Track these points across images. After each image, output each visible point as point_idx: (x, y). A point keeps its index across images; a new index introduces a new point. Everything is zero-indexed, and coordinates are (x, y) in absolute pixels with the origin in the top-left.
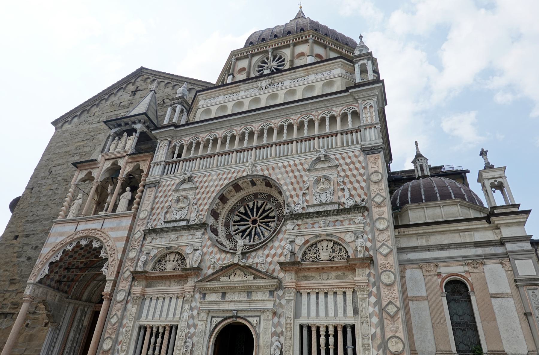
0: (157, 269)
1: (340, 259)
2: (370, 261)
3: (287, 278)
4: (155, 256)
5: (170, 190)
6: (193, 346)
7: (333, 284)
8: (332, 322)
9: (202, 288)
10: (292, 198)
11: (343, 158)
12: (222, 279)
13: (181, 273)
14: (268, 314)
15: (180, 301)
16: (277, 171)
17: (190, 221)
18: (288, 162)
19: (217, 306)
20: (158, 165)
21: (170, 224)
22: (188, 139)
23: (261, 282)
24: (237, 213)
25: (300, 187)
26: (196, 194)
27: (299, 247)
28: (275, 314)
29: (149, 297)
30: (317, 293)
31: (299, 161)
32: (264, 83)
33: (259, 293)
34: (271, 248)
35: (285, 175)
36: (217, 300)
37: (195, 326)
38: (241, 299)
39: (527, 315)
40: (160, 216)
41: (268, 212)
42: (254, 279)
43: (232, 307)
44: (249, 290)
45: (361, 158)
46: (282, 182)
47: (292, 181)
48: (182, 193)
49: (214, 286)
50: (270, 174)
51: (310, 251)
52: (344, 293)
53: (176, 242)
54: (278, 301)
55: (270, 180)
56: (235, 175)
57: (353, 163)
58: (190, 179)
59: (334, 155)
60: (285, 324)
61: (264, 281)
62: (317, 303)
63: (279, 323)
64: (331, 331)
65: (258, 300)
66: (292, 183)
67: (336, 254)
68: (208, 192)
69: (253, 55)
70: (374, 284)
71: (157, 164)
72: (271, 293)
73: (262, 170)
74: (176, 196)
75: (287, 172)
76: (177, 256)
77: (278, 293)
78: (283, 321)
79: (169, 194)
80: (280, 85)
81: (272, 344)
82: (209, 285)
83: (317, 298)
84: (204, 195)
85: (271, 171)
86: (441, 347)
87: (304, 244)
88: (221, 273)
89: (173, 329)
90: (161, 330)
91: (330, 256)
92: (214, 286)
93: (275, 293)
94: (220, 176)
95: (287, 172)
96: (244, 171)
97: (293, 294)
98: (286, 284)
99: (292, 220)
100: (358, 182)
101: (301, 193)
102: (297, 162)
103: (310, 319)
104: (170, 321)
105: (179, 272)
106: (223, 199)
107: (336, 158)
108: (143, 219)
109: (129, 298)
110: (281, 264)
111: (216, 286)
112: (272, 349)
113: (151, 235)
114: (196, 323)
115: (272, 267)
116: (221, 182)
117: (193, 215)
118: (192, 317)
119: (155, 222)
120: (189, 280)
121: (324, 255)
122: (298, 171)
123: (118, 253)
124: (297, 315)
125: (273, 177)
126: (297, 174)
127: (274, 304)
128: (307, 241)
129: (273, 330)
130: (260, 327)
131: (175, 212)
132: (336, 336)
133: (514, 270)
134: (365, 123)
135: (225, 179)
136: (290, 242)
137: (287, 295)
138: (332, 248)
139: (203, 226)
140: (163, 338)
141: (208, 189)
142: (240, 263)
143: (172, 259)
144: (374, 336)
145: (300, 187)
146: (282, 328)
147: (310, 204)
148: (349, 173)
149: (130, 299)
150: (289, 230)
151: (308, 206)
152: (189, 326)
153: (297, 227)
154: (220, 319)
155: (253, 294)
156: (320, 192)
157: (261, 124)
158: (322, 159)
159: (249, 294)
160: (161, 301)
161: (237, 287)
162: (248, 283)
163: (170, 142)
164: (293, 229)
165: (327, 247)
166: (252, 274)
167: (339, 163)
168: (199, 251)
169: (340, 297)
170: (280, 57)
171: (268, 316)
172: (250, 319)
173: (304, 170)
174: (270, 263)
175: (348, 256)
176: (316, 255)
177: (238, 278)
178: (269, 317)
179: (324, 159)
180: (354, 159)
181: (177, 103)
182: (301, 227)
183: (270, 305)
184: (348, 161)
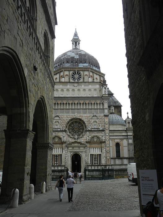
2: (105, 142)
8: (97, 153)
15: (61, 149)
16: (83, 117)
23: (82, 146)
28: (85, 152)
32: (76, 85)
37: (67, 155)
39: (129, 150)
45: (104, 117)
46: (85, 121)
48: (56, 120)
56: (72, 117)
57: (102, 118)
58: (58, 116)
64: (97, 155)
69: (70, 70)
70: (105, 147)
72: (84, 148)
73: (79, 117)
78: (87, 153)
80: (81, 86)
84: (63, 122)
86: (114, 156)
89: (61, 155)
90: (57, 155)
94: (67, 117)
104: (59, 153)
105: (60, 142)
106: (68, 123)
115: (84, 142)
116: (68, 118)
121: (95, 140)
124: (90, 152)
126: (88, 119)
132: (97, 156)
133: (128, 141)
139: (65, 131)
140: (58, 157)
144: (105, 156)
148: (101, 121)
169: (98, 149)
170: (79, 74)
177: (76, 145)
180: (102, 117)
183: (84, 150)
184: (101, 117)
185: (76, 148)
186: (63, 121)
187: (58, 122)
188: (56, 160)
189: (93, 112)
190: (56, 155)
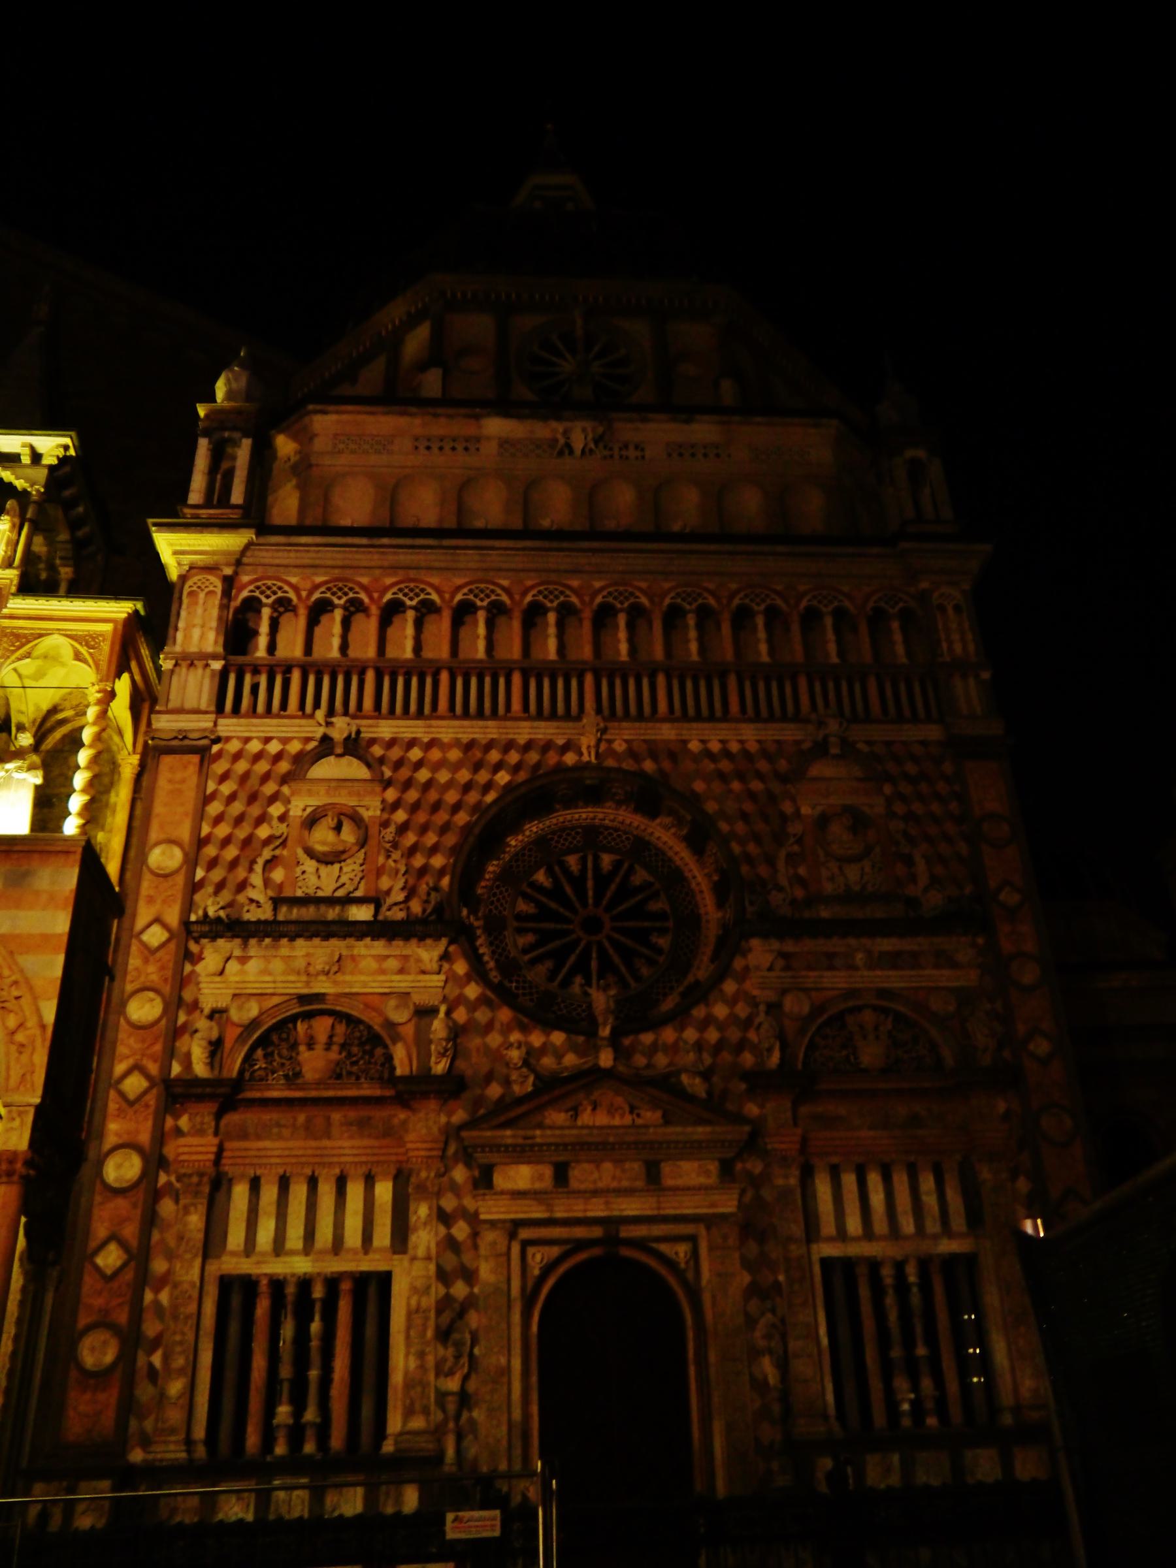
0: (262, 1073)
4: (254, 1023)
5: (266, 778)
17: (384, 908)
19: (543, 1208)
20: (192, 665)
21: (303, 911)
22: (308, 585)
23: (700, 1132)
24: (525, 887)
29: (243, 1176)
35: (717, 786)
36: (538, 1186)
37: (469, 1276)
38: (625, 1184)
40: (241, 873)
41: (639, 897)
43: (597, 1209)
45: (948, 768)
46: (711, 807)
49: (529, 1142)
53: (339, 977)
56: (533, 757)
59: (869, 743)
61: (708, 1129)
65: (688, 1189)
66: (745, 816)
68: (436, 807)
71: (190, 660)
74: (302, 806)
75: (722, 776)
76: (341, 1029)
77: (749, 1166)
79: (270, 788)
80: (632, 453)
84: (421, 817)
85: (667, 765)
90: (318, 1292)
92: (529, 1142)
93: (739, 1166)
95: (722, 776)
96: (565, 748)
97: (796, 1172)
101: (782, 854)
102: (753, 747)
108: (166, 876)
109: (163, 1179)
111: (538, 1140)
113: (221, 942)
116: (483, 777)
117: (394, 886)
118: (451, 1244)
119: (226, 896)
122: (760, 776)
123: (35, 999)
124: (812, 1232)
126: (756, 786)
127: (739, 1201)
131: (310, 865)
134: (948, 659)
135: (498, 767)
141: (433, 796)
142: (621, 1068)
143: (322, 1038)
149: (169, 1184)
152: (443, 1276)
153: (780, 963)
154: (555, 1251)
155: (666, 1168)
157: (602, 589)
160: (299, 1193)
163: (229, 583)
164: (770, 969)
172: (664, 1248)
176: (844, 1053)
181: (234, 429)
184: (911, 768)
185: (607, 1174)
190: (305, 1283)
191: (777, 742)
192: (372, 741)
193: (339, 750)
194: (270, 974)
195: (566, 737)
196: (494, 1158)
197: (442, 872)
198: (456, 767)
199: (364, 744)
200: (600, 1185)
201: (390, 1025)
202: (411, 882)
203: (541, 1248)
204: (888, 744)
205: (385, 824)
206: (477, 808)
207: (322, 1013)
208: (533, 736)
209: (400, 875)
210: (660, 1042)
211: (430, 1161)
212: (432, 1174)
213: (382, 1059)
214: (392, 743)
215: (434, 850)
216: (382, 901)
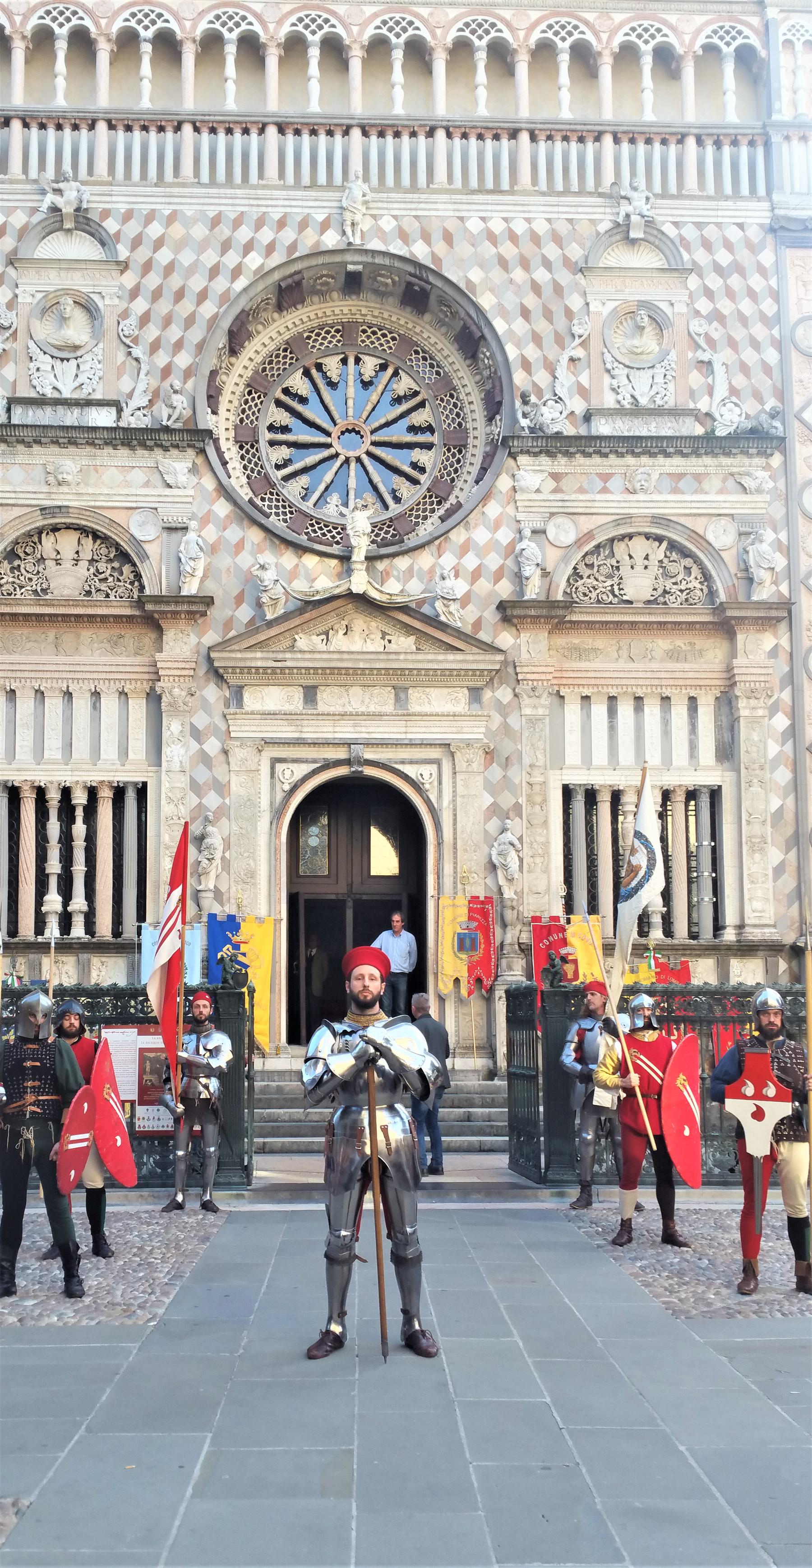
1: (687, 600)
3: (524, 650)
6: (227, 846)
7: (663, 675)
9: (233, 668)
10: (530, 373)
11: (707, 245)
12: (302, 642)
13: (128, 612)
14: (470, 754)
16: (463, 249)
17: (126, 412)
18: (506, 220)
19: (293, 728)
23: (451, 660)
25: (556, 333)
26: (127, 295)
27: (559, 553)
28: (490, 754)
30: (612, 699)
31: (547, 226)
33: (434, 693)
34: (465, 549)
35: (497, 275)
36: (287, 708)
37: (222, 789)
38: (372, 708)
42: (418, 649)
43: (346, 731)
44: (400, 683)
45: (767, 258)
46: (486, 301)
47: (526, 302)
50: (435, 258)
51: (590, 566)
52: (693, 700)
54: (497, 719)
55: (439, 283)
56: (288, 235)
59: (676, 224)
60: (524, 784)
61: (459, 657)
62: (612, 728)
63: (506, 783)
67: (675, 584)
68: (180, 295)
72: (475, 693)
73: (404, 236)
75: (503, 263)
78: (517, 775)
81: (490, 840)
82: (262, 659)
83: (612, 712)
84: (164, 306)
85: (440, 248)
87: (579, 542)
88: (297, 621)
90: (80, 798)
91: (655, 589)
92: (279, 664)
93: (487, 695)
94: (224, 231)
95: (503, 263)
96: (325, 226)
97: (545, 700)
98: (525, 670)
99: (536, 455)
100: (755, 345)
102: (541, 227)
103: (592, 772)
107: (682, 239)
110: (502, 606)
111: (289, 664)
112: (494, 852)
114: (223, 779)
116: (232, 259)
120: (164, 637)
122: (547, 264)
125: (454, 279)
126: (541, 275)
127: (487, 727)
128: (590, 535)
129: (488, 800)
130: (440, 791)
135: (248, 248)
136: (534, 532)
137: (526, 700)
138: (661, 562)
141: (175, 282)
145: (556, 333)
146: (515, 796)
147: (595, 404)
148: (725, 306)
150: (523, 490)
151: (587, 418)
152: (196, 787)
153: (551, 484)
154: (306, 769)
155: (414, 694)
156: (627, 363)
158: (633, 235)
159: (402, 696)
160: (54, 705)
161: (363, 669)
162: (405, 660)
164: (538, 491)
165: (647, 558)
166: (409, 630)
167: (694, 263)
168: (191, 536)
169: (679, 712)
171: (469, 762)
173: (567, 262)
174: (465, 601)
175: (712, 594)
176: (609, 583)
178: (475, 766)
179: (641, 235)
180: (744, 256)
182: (564, 483)
183: (475, 731)
184: (724, 258)
186: (157, 295)
187: (88, 308)
188: (54, 866)
189: (608, 177)
191: (570, 221)
192: (106, 214)
193: (68, 225)
194: (10, 483)
195: (327, 211)
196: (245, 679)
197: (188, 373)
198: (202, 246)
199: (94, 216)
200: (349, 709)
201: (138, 543)
202: (154, 383)
203: (290, 766)
204: (699, 225)
205: (125, 314)
206: (225, 298)
207: (68, 527)
208: (288, 210)
209: (142, 375)
210: (416, 567)
211: (182, 679)
212: (184, 693)
213: (132, 576)
214: (128, 216)
215: (179, 346)
216: (124, 405)
